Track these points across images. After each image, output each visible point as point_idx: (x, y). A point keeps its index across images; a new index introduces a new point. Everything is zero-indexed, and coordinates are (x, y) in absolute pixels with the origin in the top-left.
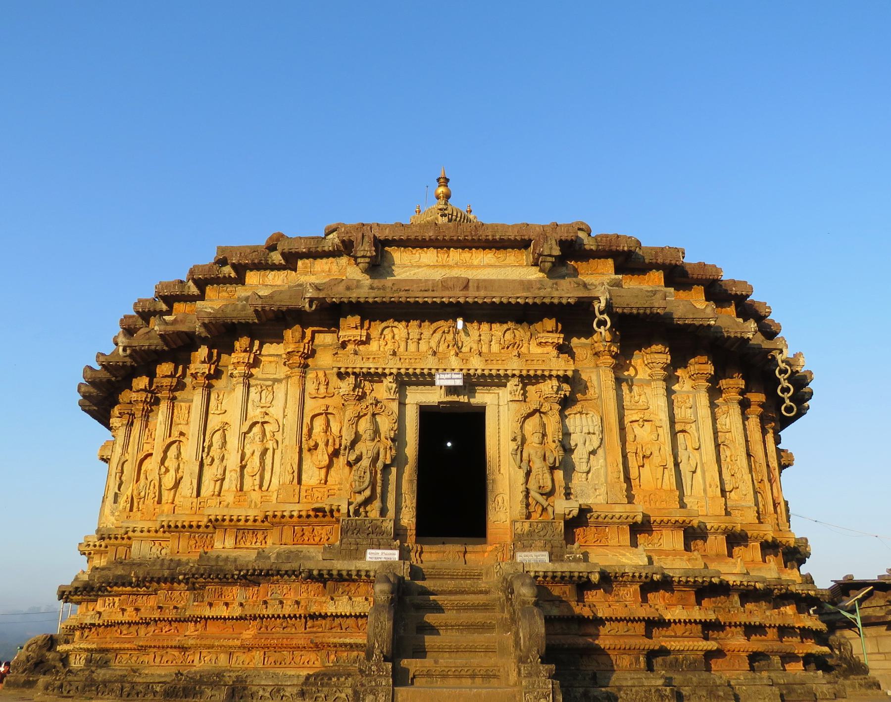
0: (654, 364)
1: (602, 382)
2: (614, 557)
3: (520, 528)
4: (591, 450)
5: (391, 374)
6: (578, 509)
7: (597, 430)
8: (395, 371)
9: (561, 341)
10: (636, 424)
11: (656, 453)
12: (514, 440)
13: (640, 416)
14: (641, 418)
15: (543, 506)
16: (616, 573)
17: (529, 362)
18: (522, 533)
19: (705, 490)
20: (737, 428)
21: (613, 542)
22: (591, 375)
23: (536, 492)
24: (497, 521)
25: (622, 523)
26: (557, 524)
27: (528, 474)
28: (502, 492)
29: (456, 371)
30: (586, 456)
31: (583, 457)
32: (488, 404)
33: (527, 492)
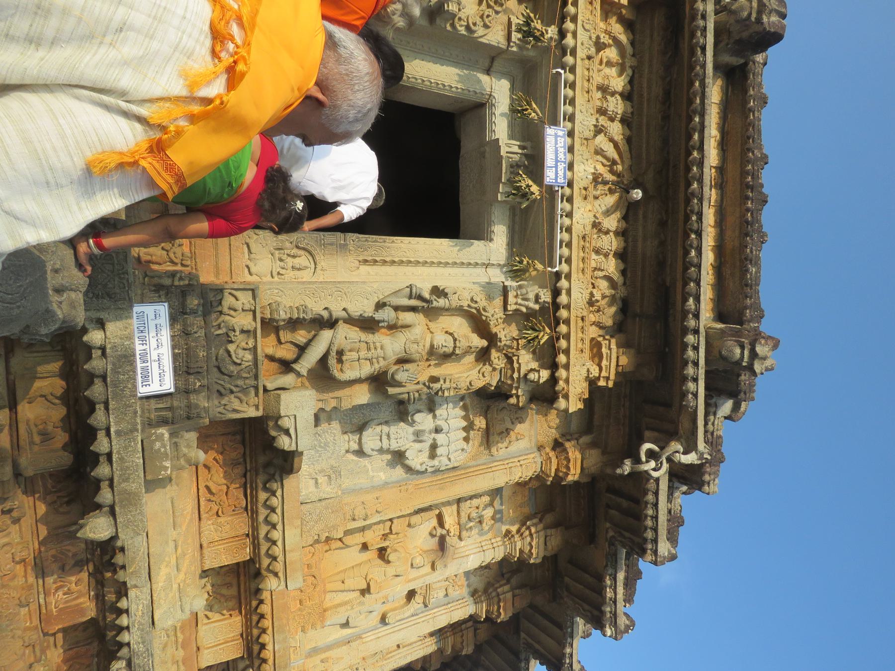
0: (529, 539)
1: (516, 460)
2: (172, 545)
3: (238, 305)
4: (407, 454)
5: (562, 34)
6: (293, 448)
7: (441, 462)
8: (569, 41)
9: (602, 383)
10: (434, 522)
11: (391, 570)
12: (438, 292)
13: (452, 530)
14: (448, 531)
15: (296, 361)
16: (123, 567)
17: (580, 323)
18: (225, 310)
19: (315, 651)
20: (405, 657)
21: (209, 528)
22: (527, 439)
23: (331, 343)
24: (250, 252)
25: (256, 546)
26: (253, 400)
27: (368, 324)
28: (319, 267)
29: (569, 174)
30: (394, 446)
31: (393, 441)
32: (491, 244)
33: (332, 324)
